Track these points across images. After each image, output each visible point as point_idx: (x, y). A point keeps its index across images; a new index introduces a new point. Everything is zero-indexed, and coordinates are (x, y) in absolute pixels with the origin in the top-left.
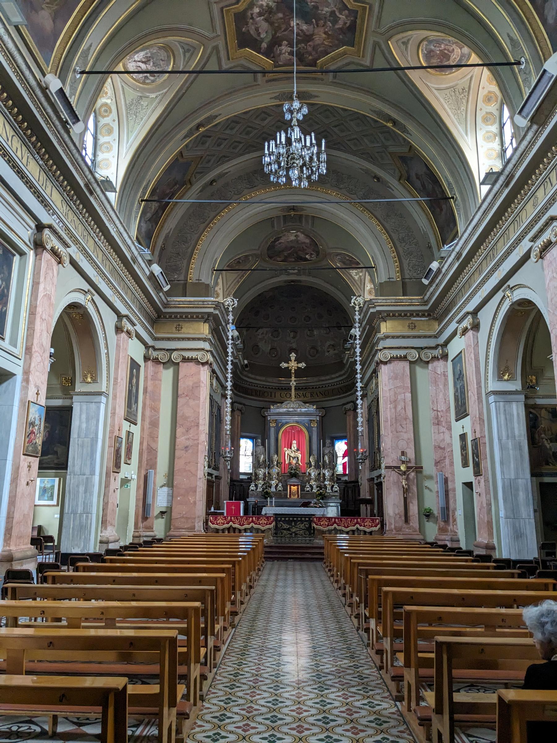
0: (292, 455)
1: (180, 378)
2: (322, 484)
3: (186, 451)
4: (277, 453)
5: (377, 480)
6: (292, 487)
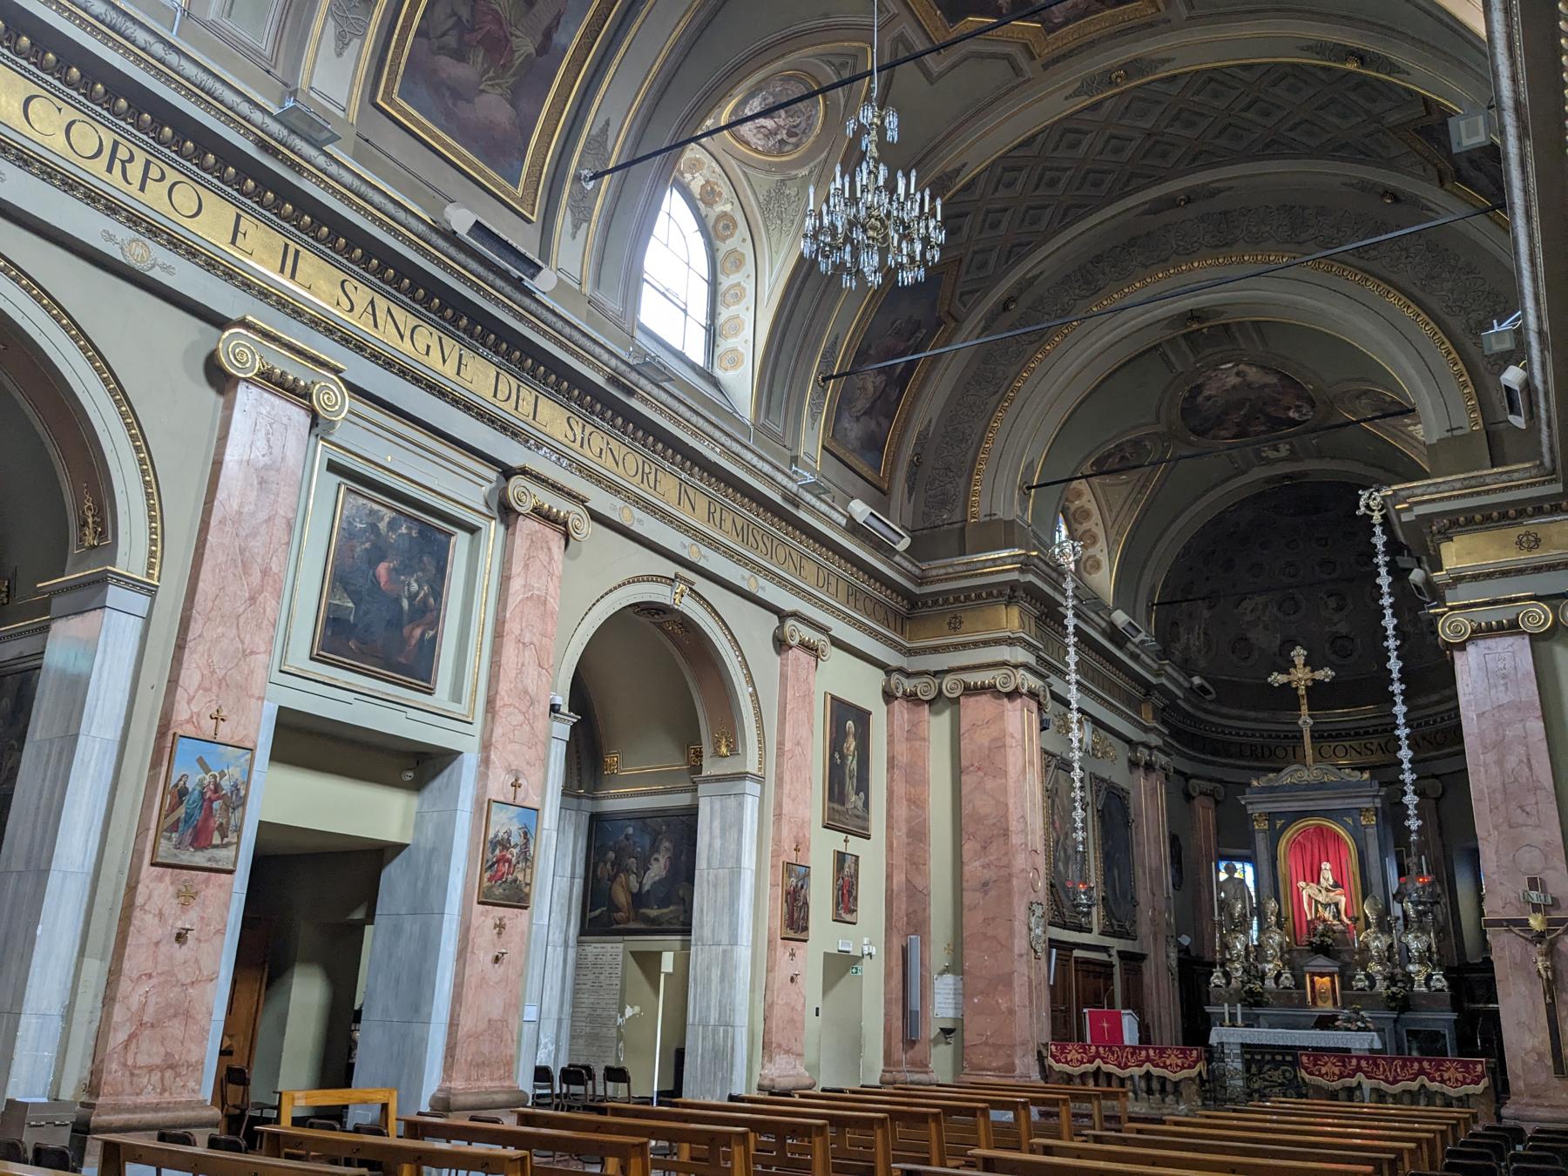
1: (962, 731)
2: (1398, 970)
3: (986, 893)
6: (1316, 978)
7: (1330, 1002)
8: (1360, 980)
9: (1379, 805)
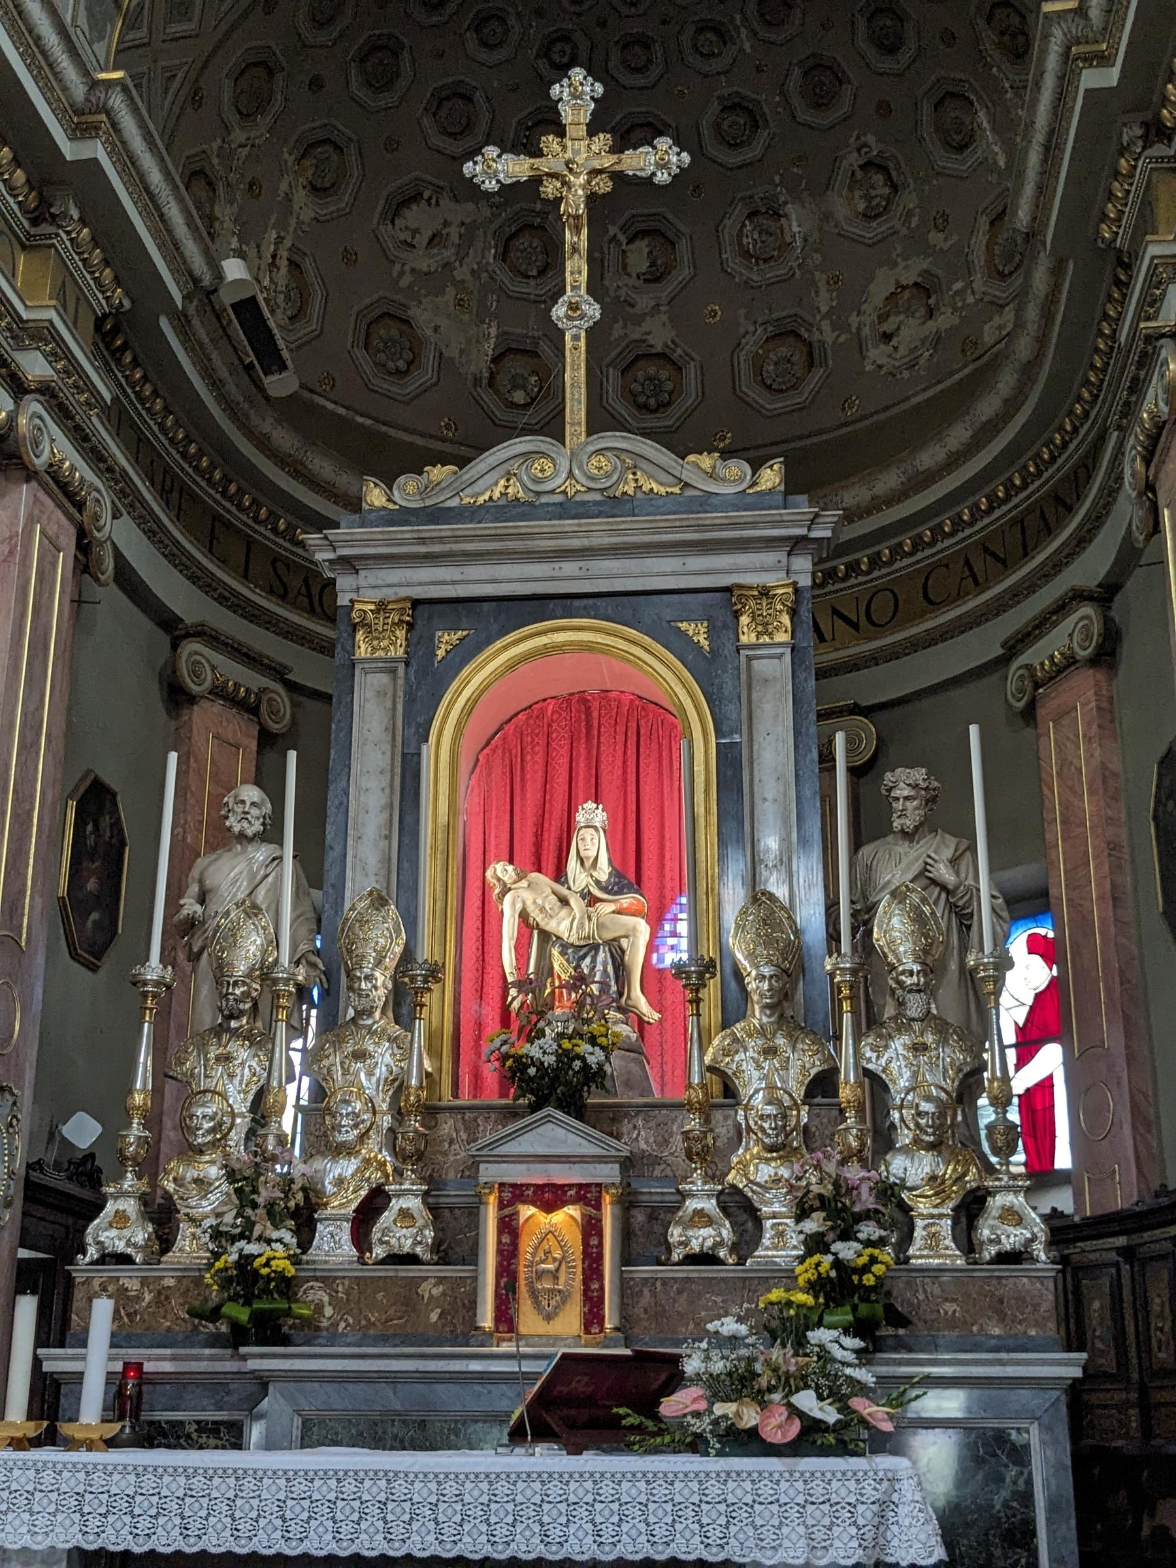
0: (563, 925)
2: (853, 1172)
6: (527, 1211)
7: (570, 1321)
8: (701, 1218)
9: (805, 581)
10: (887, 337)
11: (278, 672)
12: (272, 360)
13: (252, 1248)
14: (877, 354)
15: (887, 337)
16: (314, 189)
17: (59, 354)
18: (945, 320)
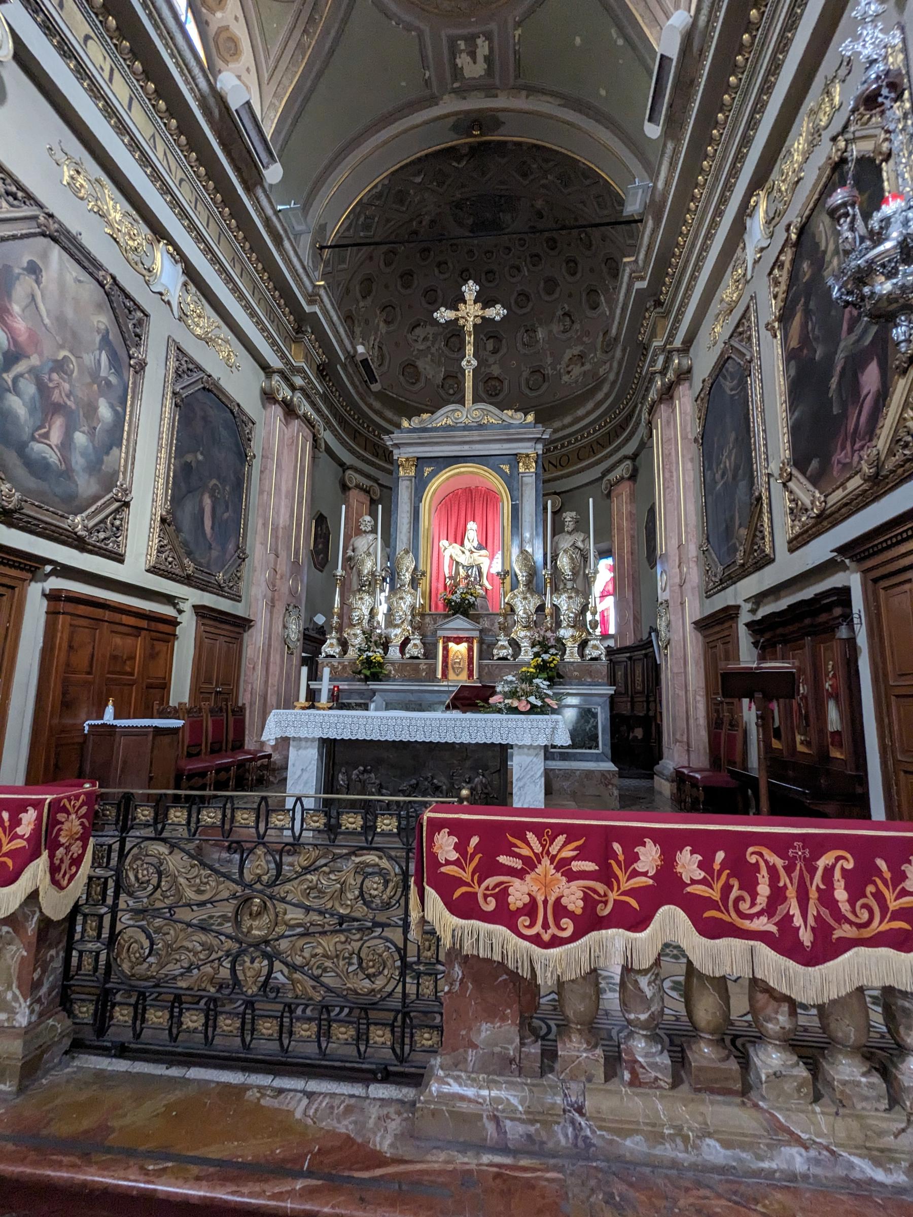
2: (549, 634)
4: (414, 548)
5: (753, 611)
7: (464, 676)
8: (503, 647)
9: (540, 452)
10: (569, 372)
11: (376, 480)
12: (373, 379)
13: (370, 654)
14: (566, 378)
15: (569, 372)
16: (385, 321)
17: (306, 377)
18: (587, 367)
